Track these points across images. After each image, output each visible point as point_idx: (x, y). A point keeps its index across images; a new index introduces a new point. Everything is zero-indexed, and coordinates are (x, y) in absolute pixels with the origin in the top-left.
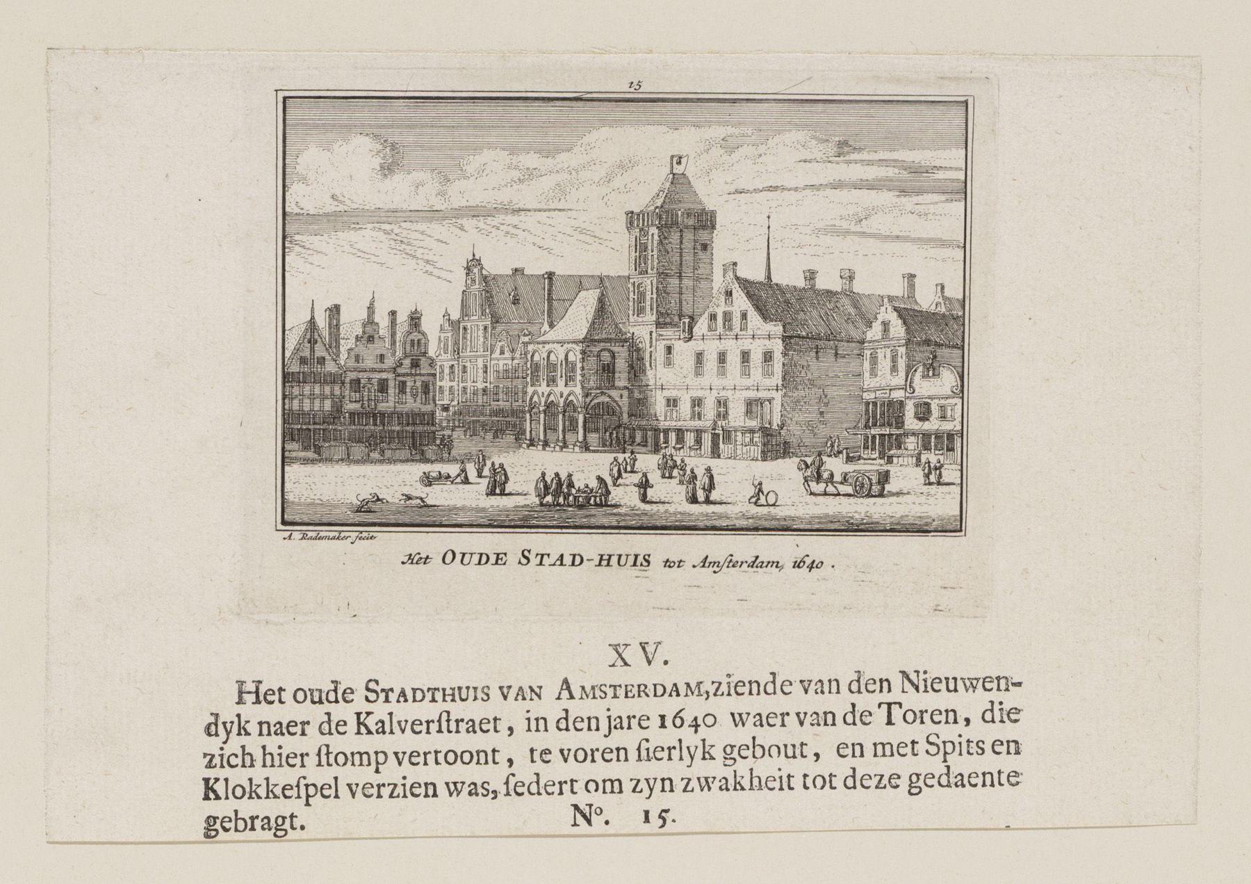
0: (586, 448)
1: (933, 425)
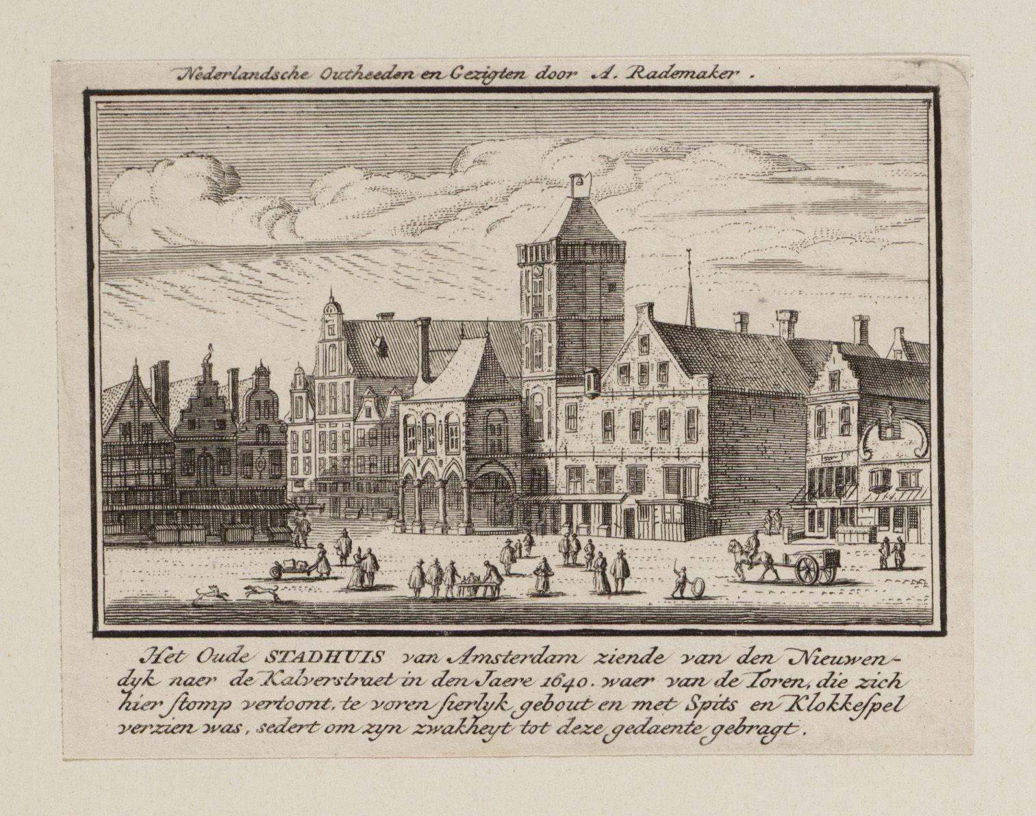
0: (470, 531)
1: (895, 495)
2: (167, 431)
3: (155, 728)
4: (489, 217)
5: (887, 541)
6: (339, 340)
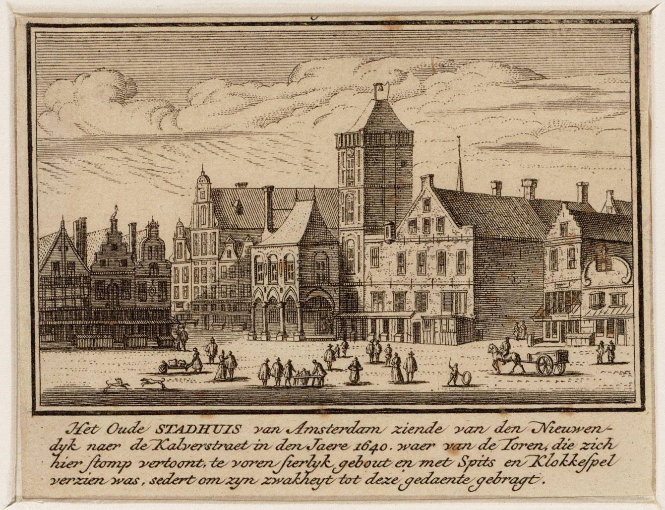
2: (86, 268)
3: (76, 480)
4: (315, 114)
5: (602, 343)
6: (208, 202)
